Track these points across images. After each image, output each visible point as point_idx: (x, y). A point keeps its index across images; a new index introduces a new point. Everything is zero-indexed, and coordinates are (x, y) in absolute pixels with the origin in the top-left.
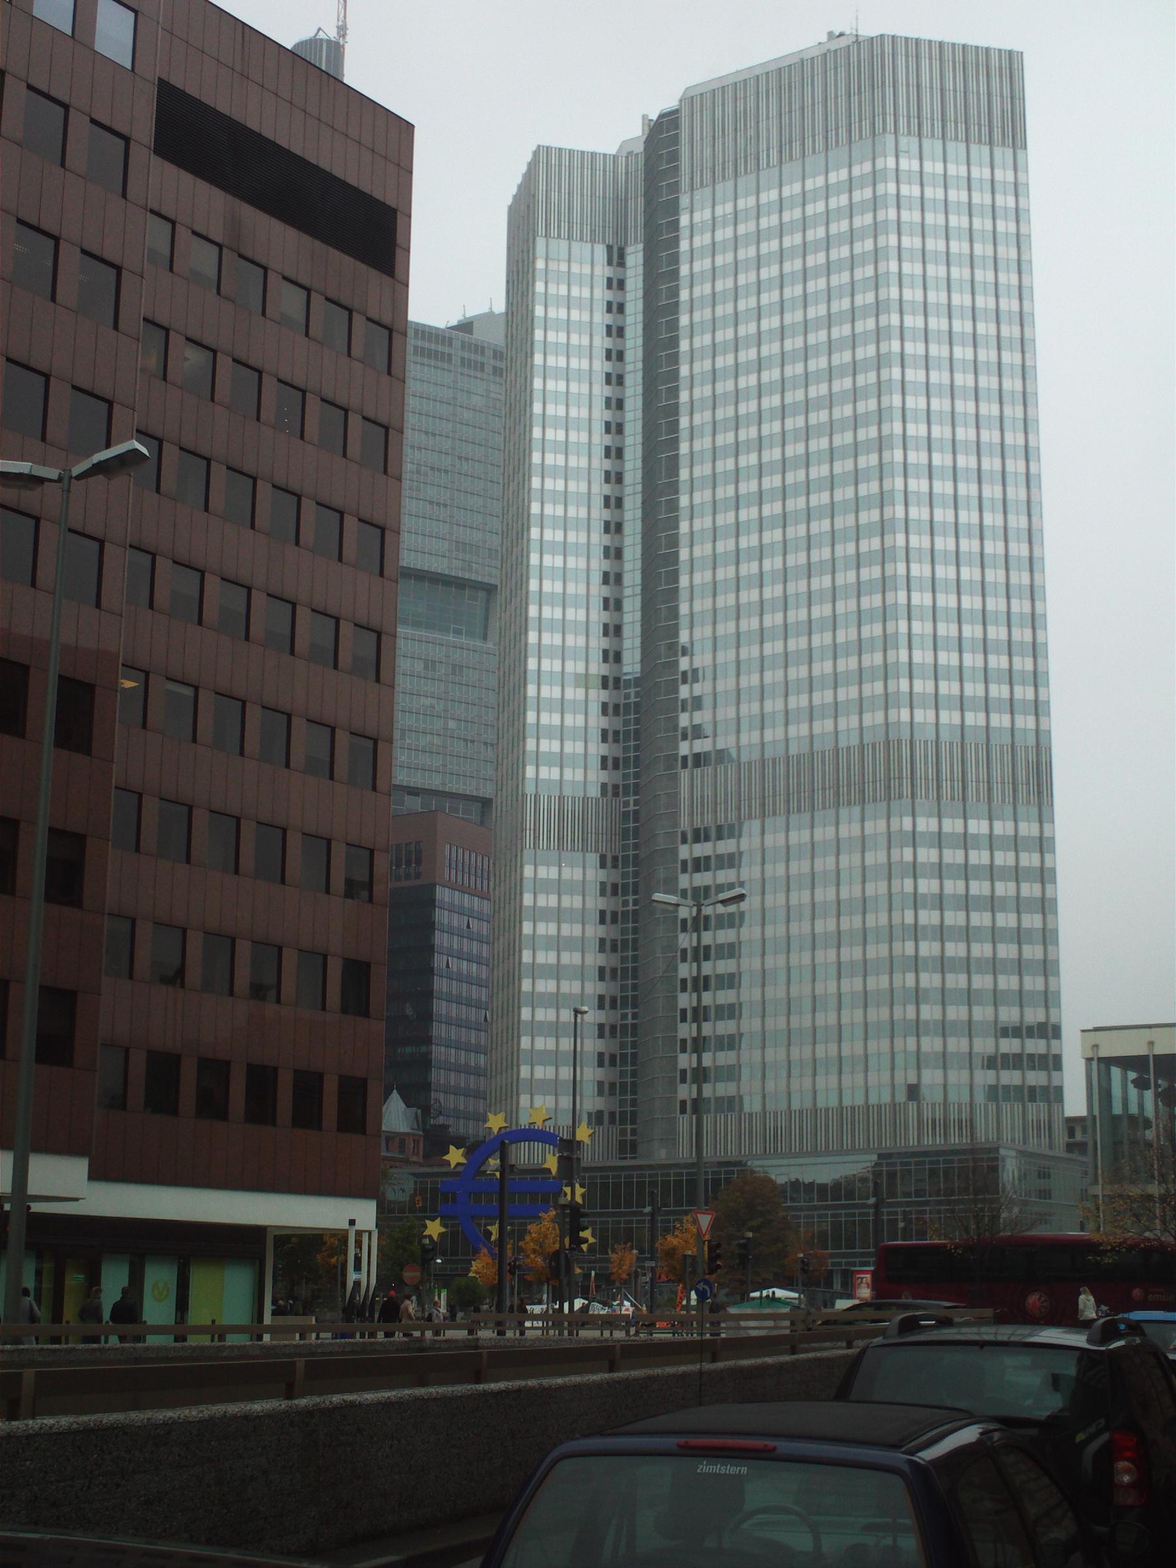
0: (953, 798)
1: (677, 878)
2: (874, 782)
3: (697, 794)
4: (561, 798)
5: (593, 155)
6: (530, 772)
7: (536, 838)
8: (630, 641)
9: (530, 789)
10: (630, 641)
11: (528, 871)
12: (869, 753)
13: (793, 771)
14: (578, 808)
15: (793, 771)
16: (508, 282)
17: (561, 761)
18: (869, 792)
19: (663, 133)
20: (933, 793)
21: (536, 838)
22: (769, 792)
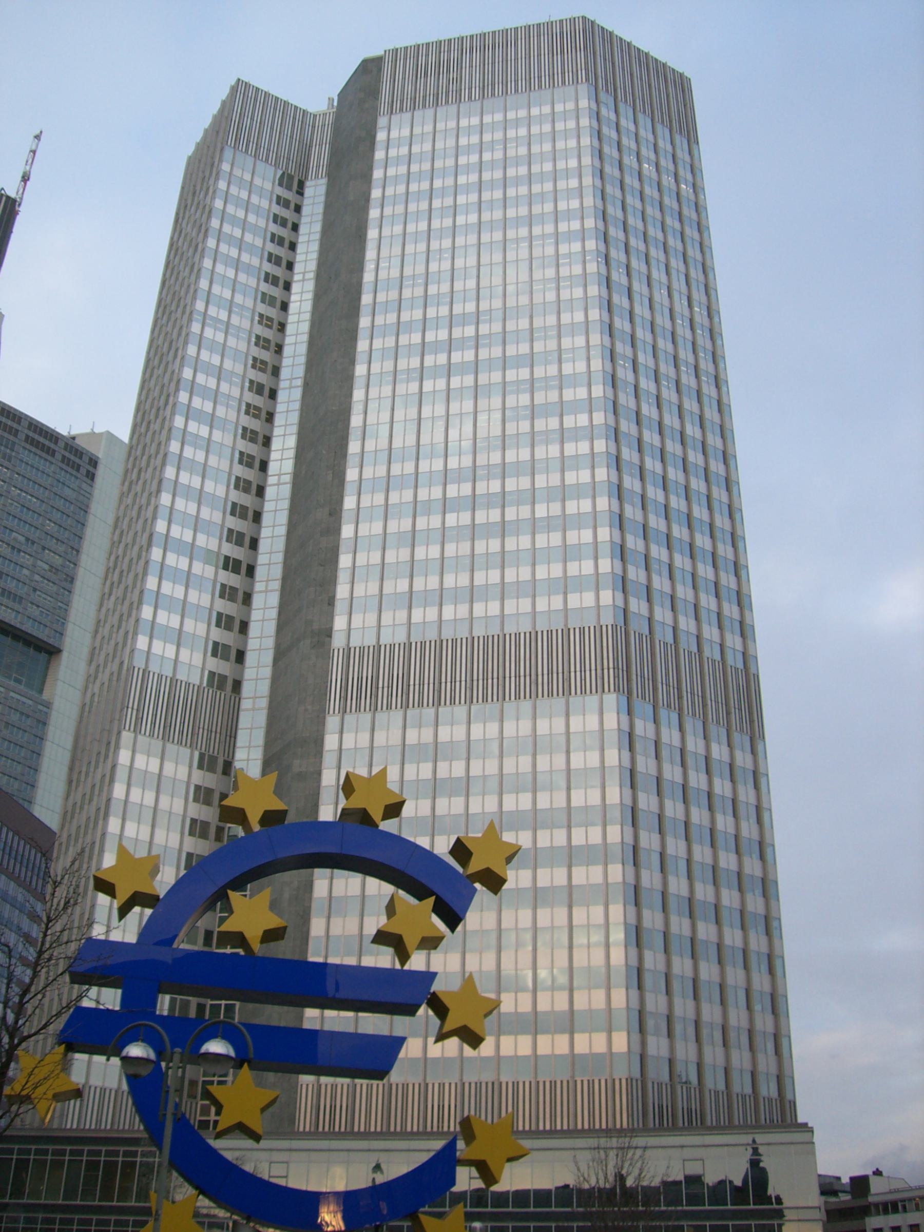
0: (669, 706)
1: (319, 774)
2: (583, 670)
3: (354, 674)
4: (174, 681)
5: (286, 103)
6: (142, 642)
7: (139, 719)
8: (277, 522)
9: (139, 663)
10: (277, 522)
11: (124, 757)
12: (575, 638)
13: (478, 655)
14: (192, 696)
15: (478, 655)
16: (183, 188)
17: (179, 637)
18: (575, 680)
19: (369, 71)
20: (649, 694)
21: (139, 719)
22: (447, 676)
